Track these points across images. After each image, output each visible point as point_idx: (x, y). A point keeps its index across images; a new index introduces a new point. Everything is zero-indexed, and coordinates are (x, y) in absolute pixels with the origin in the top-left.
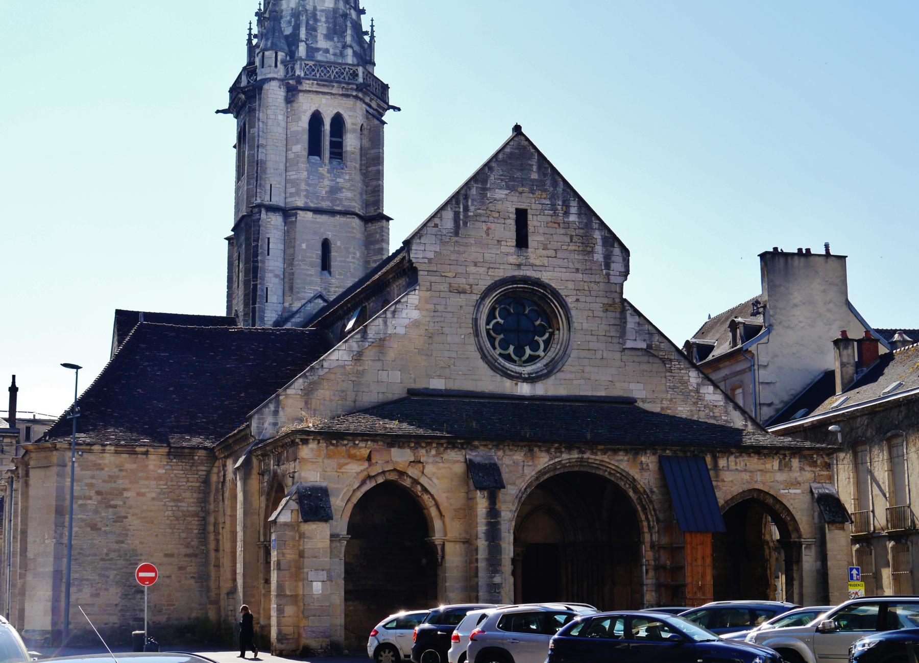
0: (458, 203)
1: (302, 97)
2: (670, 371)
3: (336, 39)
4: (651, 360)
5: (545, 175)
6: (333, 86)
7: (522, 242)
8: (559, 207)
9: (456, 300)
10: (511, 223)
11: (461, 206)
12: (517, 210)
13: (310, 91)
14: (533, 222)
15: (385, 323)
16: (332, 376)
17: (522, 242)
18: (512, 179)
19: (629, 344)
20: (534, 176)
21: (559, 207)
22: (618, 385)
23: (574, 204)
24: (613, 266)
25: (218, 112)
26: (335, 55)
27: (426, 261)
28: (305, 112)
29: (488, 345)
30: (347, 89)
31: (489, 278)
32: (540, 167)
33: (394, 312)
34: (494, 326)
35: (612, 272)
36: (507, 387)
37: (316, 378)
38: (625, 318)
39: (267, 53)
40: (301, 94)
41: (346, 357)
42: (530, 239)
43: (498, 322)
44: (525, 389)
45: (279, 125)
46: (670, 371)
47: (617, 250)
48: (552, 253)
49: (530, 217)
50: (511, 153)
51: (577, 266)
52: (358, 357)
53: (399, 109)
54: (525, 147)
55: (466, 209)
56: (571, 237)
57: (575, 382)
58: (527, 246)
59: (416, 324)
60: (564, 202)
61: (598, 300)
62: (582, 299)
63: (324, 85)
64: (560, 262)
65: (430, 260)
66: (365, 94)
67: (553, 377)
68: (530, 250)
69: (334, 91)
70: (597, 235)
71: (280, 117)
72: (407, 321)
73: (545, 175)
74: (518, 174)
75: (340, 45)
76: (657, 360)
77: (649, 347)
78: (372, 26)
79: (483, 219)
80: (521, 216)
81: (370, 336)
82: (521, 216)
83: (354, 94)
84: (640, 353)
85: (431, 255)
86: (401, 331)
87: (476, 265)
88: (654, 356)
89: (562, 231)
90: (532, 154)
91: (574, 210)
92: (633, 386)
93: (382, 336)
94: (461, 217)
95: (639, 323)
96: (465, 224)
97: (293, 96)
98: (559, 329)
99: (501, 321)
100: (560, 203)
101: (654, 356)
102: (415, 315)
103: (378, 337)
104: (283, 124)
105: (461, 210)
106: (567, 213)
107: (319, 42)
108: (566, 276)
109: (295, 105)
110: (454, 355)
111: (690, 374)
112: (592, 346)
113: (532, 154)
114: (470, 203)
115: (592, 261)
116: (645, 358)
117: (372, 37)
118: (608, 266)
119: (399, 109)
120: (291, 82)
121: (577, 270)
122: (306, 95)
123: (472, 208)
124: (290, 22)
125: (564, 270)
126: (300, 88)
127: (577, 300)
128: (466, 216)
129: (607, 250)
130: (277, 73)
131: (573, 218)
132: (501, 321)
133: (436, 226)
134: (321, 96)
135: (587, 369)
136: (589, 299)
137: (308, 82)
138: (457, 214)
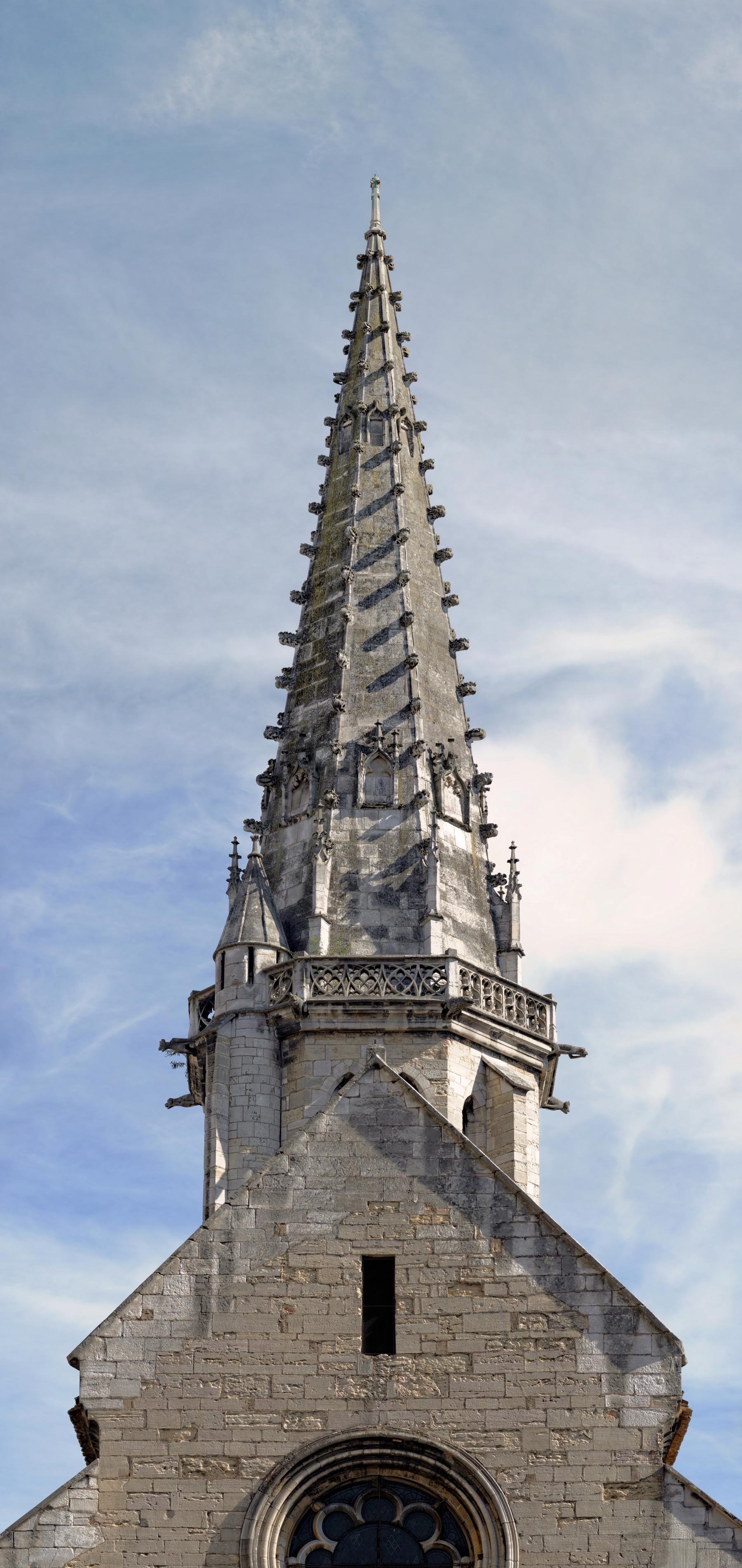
0: (205, 1254)
1: (310, 1048)
3: (404, 902)
5: (444, 1163)
6: (386, 1014)
7: (379, 1336)
11: (215, 1262)
12: (367, 1261)
13: (331, 1032)
14: (403, 1287)
17: (379, 1336)
18: (354, 1180)
23: (525, 1229)
25: (171, 1103)
26: (401, 939)
28: (320, 1081)
30: (422, 1017)
31: (284, 1436)
32: (430, 1146)
33: (34, 1532)
34: (309, 1557)
35: (628, 1400)
39: (230, 954)
40: (309, 1040)
42: (400, 1330)
43: (320, 1549)
45: (257, 1119)
47: (645, 1341)
48: (460, 1362)
49: (399, 1274)
51: (528, 1391)
53: (582, 1053)
54: (389, 1099)
55: (227, 1269)
58: (390, 1349)
62: (543, 1475)
63: (362, 1014)
64: (480, 1384)
65: (130, 1402)
66: (470, 1023)
69: (389, 1026)
70: (591, 1306)
71: (261, 1100)
73: (444, 1163)
75: (413, 915)
78: (513, 861)
79: (273, 1289)
80: (379, 1275)
82: (379, 1275)
83: (440, 1025)
85: (133, 1389)
87: (250, 1408)
89: (490, 1304)
90: (409, 1115)
91: (524, 1247)
94: (215, 1285)
95: (706, 1525)
96: (224, 1302)
97: (293, 1046)
98: (481, 1557)
99: (330, 1545)
104: (269, 1116)
105: (215, 1271)
107: (363, 914)
108: (494, 1420)
109: (296, 1066)
113: (409, 1115)
114: (237, 1253)
115: (572, 1378)
117: (515, 887)
119: (582, 1053)
120: (283, 1013)
122: (322, 1041)
123: (243, 1265)
124: (298, 876)
125: (495, 1404)
126: (304, 1025)
127: (530, 1478)
129: (617, 1342)
130: (253, 996)
132: (330, 1545)
133: (148, 1314)
134: (358, 1039)
136: (559, 1474)
137: (321, 1009)
138: (202, 1283)
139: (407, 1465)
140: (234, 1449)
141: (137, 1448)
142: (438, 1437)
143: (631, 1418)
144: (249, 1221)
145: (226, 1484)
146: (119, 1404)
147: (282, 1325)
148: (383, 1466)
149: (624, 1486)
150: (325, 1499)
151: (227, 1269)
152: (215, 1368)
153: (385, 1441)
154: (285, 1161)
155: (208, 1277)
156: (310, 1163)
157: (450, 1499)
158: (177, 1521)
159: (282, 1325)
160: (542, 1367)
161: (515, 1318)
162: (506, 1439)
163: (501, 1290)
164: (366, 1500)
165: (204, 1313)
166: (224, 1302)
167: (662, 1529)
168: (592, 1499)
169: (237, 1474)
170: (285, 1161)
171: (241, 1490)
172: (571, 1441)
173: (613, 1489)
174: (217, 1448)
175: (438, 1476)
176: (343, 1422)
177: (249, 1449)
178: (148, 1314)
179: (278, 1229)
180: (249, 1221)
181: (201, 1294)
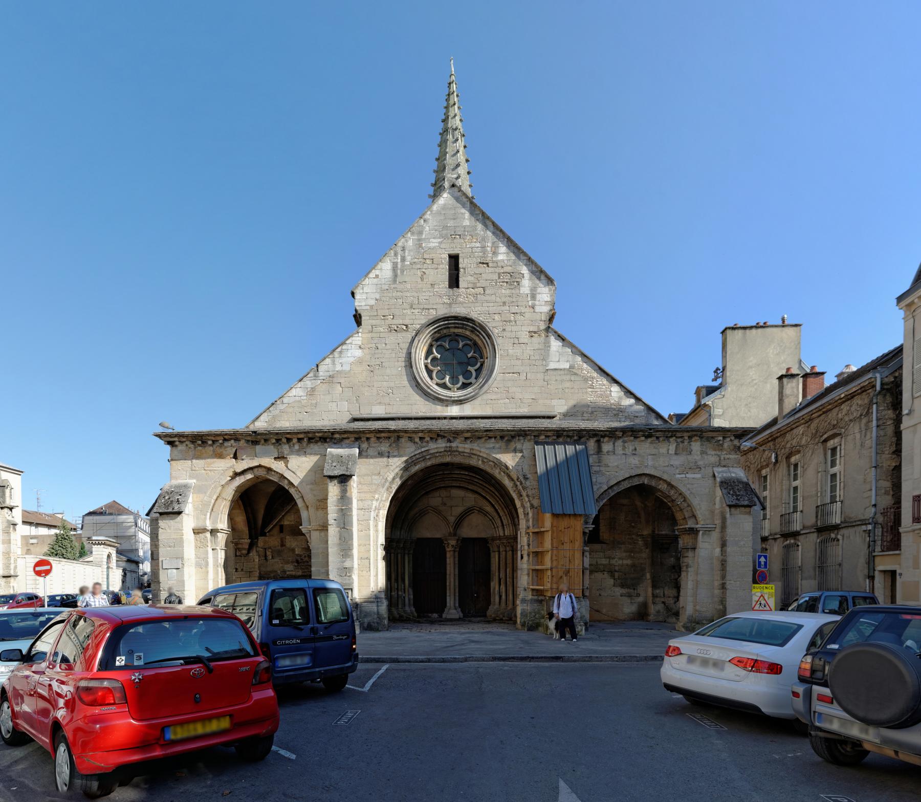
0: (396, 255)
2: (592, 387)
4: (573, 378)
7: (454, 282)
8: (489, 249)
9: (392, 339)
10: (444, 268)
12: (451, 256)
15: (334, 363)
16: (291, 410)
17: (454, 282)
18: (445, 227)
19: (552, 366)
20: (467, 223)
21: (489, 249)
22: (541, 401)
24: (538, 297)
27: (368, 307)
29: (425, 374)
33: (341, 352)
35: (537, 303)
36: (439, 410)
37: (277, 412)
38: (549, 342)
41: (301, 394)
44: (454, 411)
46: (592, 387)
49: (461, 260)
50: (445, 205)
51: (504, 299)
52: (312, 392)
55: (403, 259)
56: (499, 274)
57: (502, 401)
58: (458, 287)
59: (360, 361)
60: (493, 243)
61: (524, 328)
62: (508, 328)
64: (487, 298)
65: (372, 307)
67: (479, 399)
68: (461, 290)
72: (352, 360)
74: (451, 223)
76: (577, 378)
77: (572, 367)
79: (419, 266)
80: (454, 260)
81: (321, 373)
82: (454, 260)
84: (562, 372)
85: (373, 302)
86: (346, 368)
87: (411, 307)
88: (576, 374)
89: (491, 270)
92: (555, 402)
93: (331, 373)
96: (402, 272)
100: (489, 244)
101: (576, 374)
102: (358, 353)
103: (328, 374)
106: (495, 253)
108: (492, 310)
110: (392, 384)
111: (612, 389)
112: (516, 369)
116: (568, 377)
118: (533, 297)
121: (504, 303)
123: (408, 258)
125: (492, 304)
127: (504, 330)
128: (403, 266)
131: (500, 257)
133: (377, 276)
135: (511, 390)
136: (514, 328)
139: (463, 327)
140: (406, 322)
141: (374, 322)
142: (474, 315)
143: (537, 309)
144: (410, 243)
145: (404, 334)
146: (368, 307)
147: (422, 279)
148: (455, 327)
149: (535, 332)
150: (437, 340)
151: (403, 259)
152: (399, 294)
153: (456, 318)
154: (422, 221)
155: (397, 263)
156: (430, 221)
157: (477, 339)
158: (388, 347)
159: (422, 279)
160: (508, 291)
161: (499, 274)
162: (497, 317)
163: (495, 265)
164: (450, 341)
165: (396, 276)
166: (402, 272)
167: (547, 346)
168: (524, 337)
169: (407, 331)
170: (422, 221)
171: (409, 336)
172: (518, 317)
173: (532, 334)
174: (401, 322)
175: (473, 330)
176: (443, 311)
177: (411, 322)
178: (377, 276)
179: (420, 246)
180: (410, 243)
181: (395, 268)
